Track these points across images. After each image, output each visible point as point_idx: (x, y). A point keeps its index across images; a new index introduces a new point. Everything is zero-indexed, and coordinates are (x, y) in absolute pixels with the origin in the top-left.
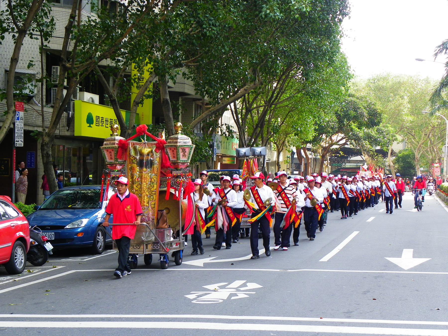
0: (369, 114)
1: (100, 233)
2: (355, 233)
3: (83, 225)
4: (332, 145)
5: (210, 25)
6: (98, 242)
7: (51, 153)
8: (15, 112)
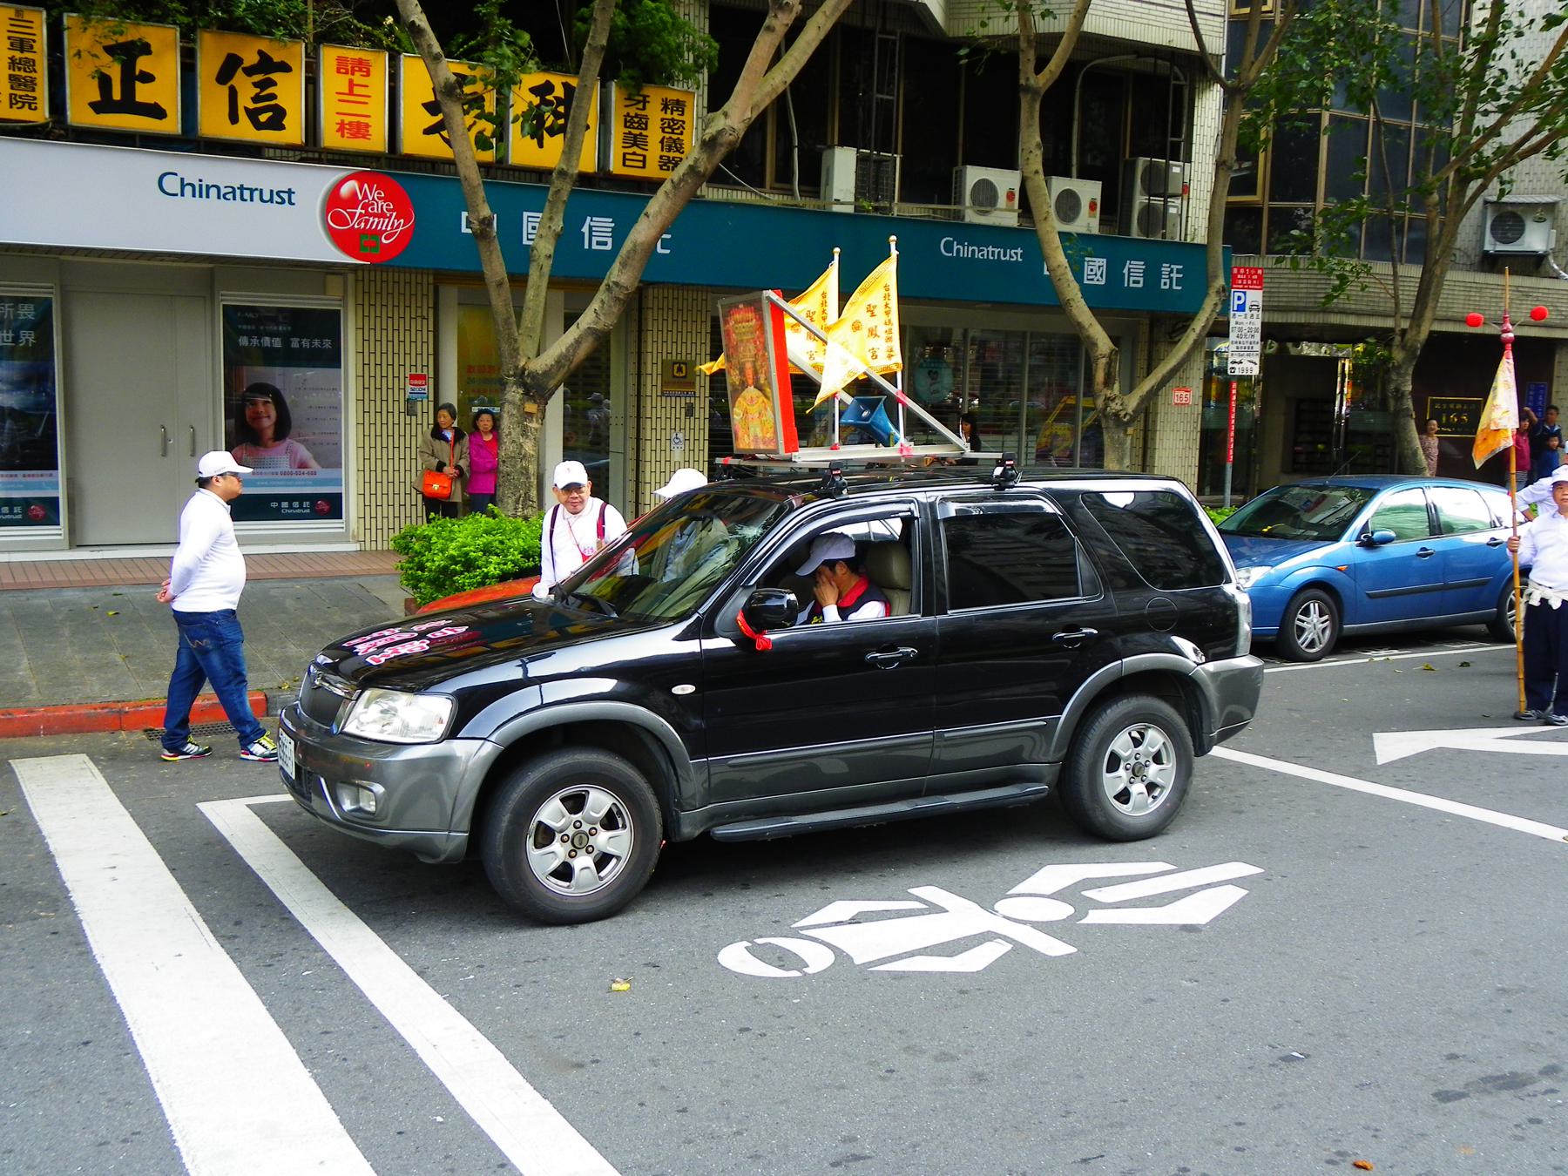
1: (1314, 607)
6: (1301, 630)
7: (1410, 388)
8: (1225, 292)
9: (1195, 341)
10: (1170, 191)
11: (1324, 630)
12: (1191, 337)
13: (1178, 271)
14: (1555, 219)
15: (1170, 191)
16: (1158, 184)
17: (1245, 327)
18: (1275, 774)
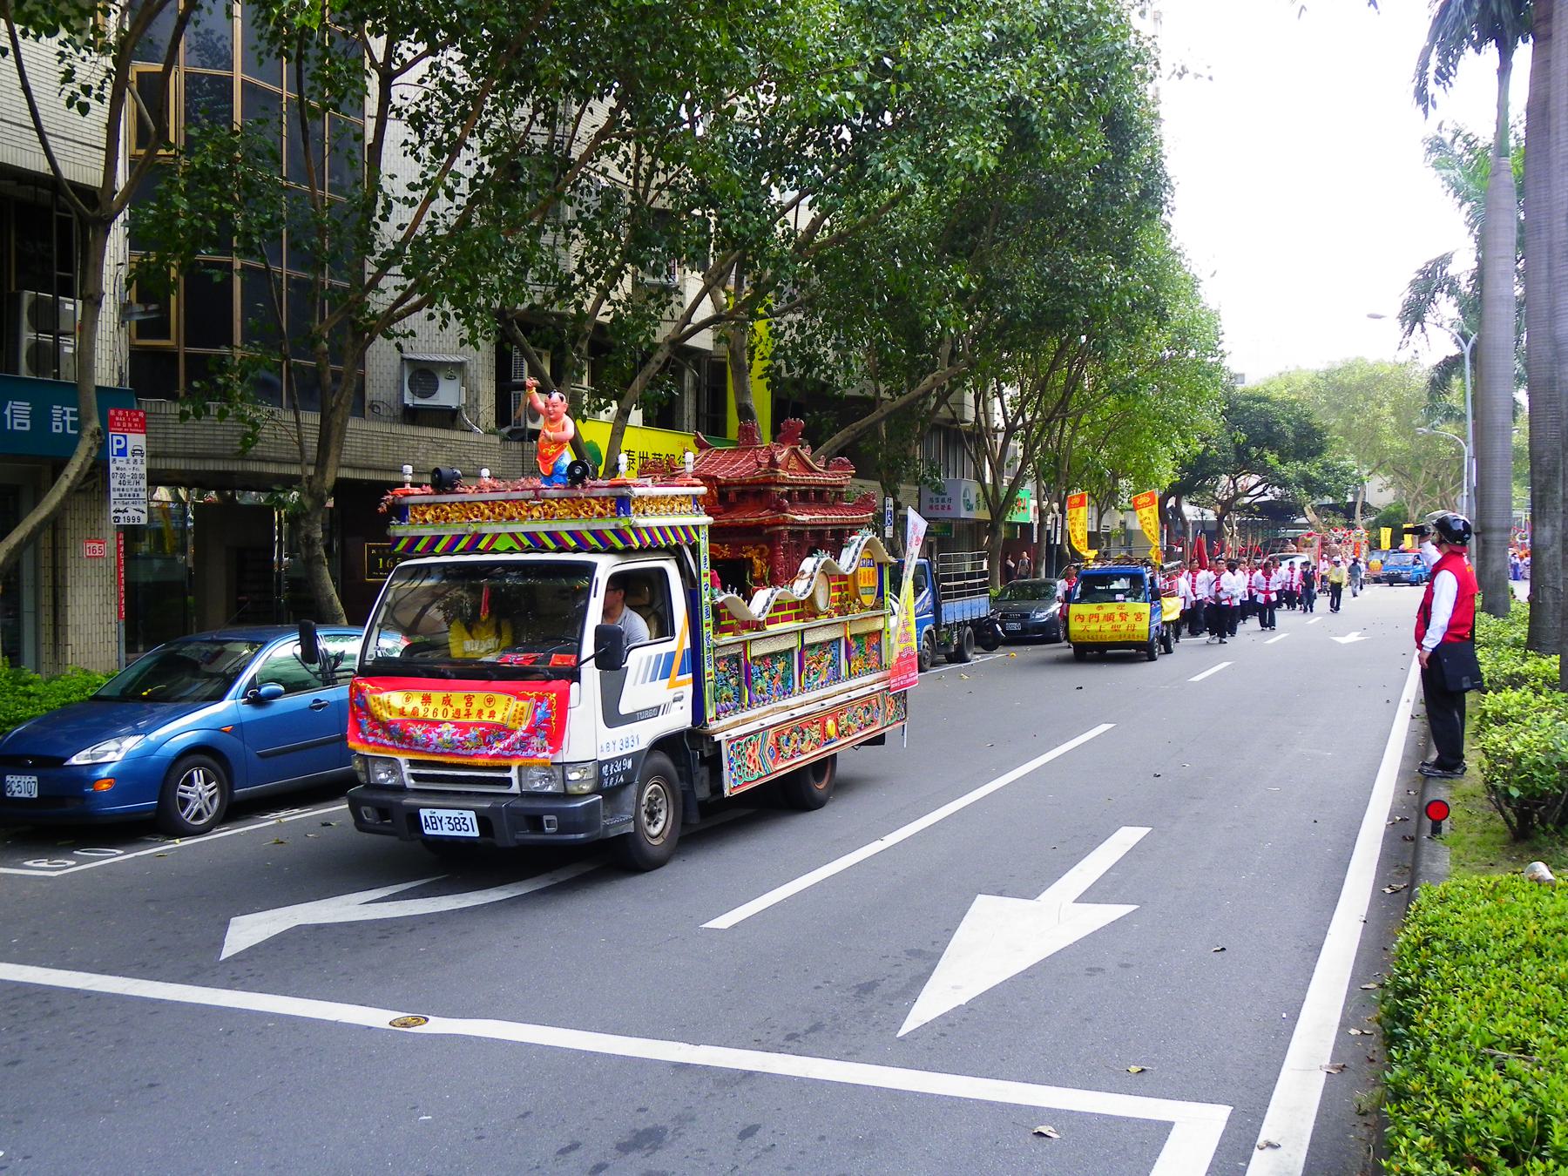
0: (1298, 436)
1: (199, 775)
2: (1104, 727)
3: (119, 757)
4: (1237, 496)
5: (740, 208)
7: (320, 535)
9: (69, 488)
10: (62, 328)
11: (211, 799)
12: (64, 483)
13: (72, 414)
14: (464, 378)
15: (62, 328)
16: (47, 319)
17: (128, 473)
18: (87, 995)
